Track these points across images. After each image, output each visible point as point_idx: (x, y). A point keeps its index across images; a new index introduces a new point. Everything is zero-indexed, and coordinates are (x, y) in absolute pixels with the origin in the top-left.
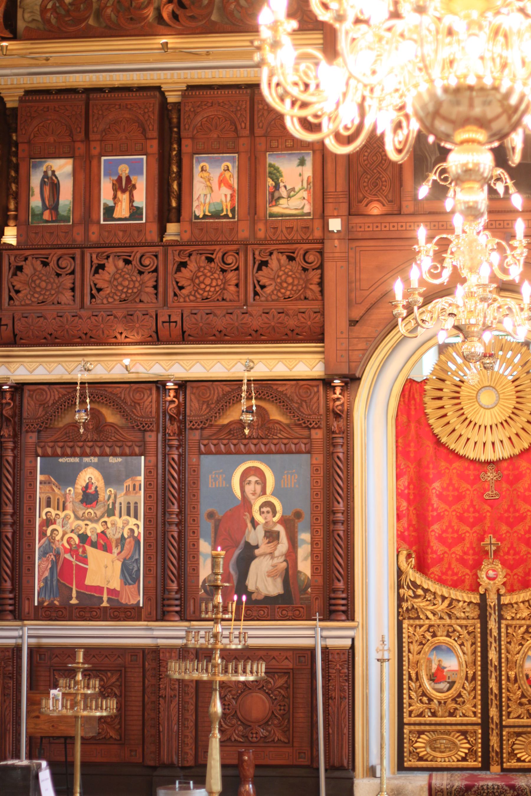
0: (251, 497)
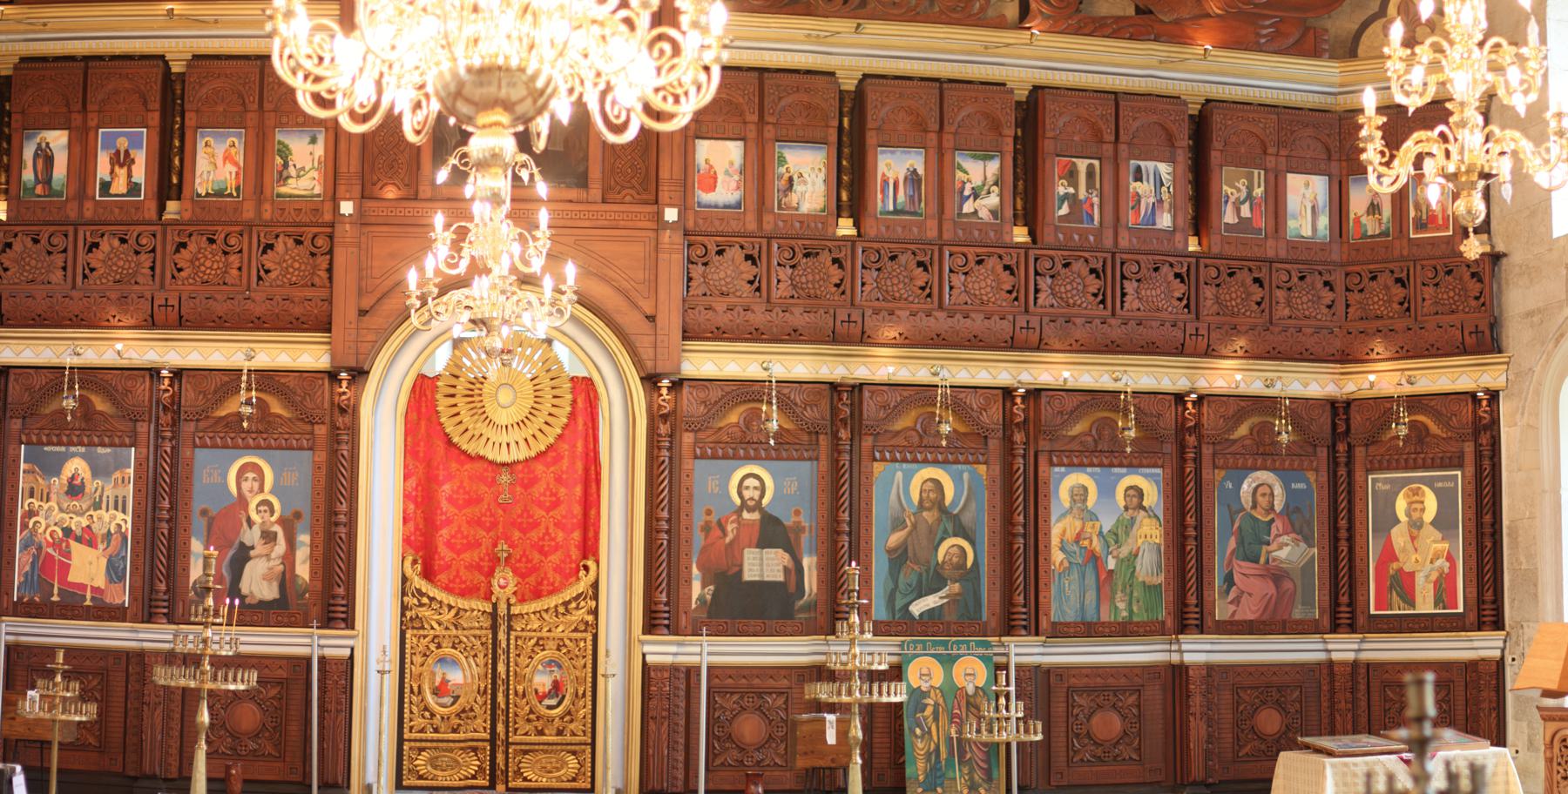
0: (248, 494)
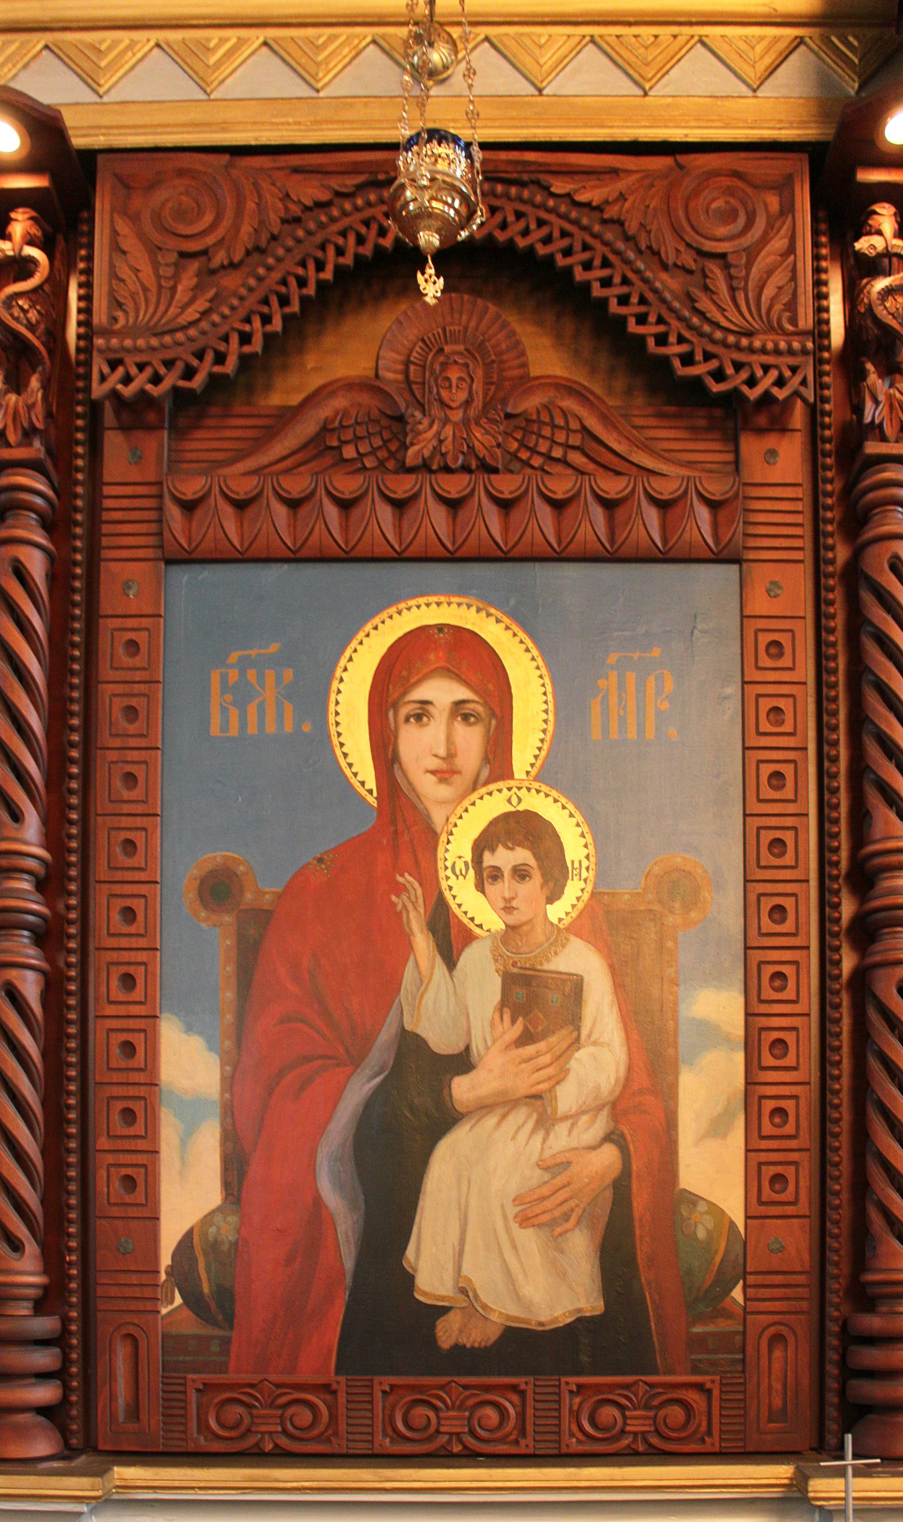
0: (430, 790)
